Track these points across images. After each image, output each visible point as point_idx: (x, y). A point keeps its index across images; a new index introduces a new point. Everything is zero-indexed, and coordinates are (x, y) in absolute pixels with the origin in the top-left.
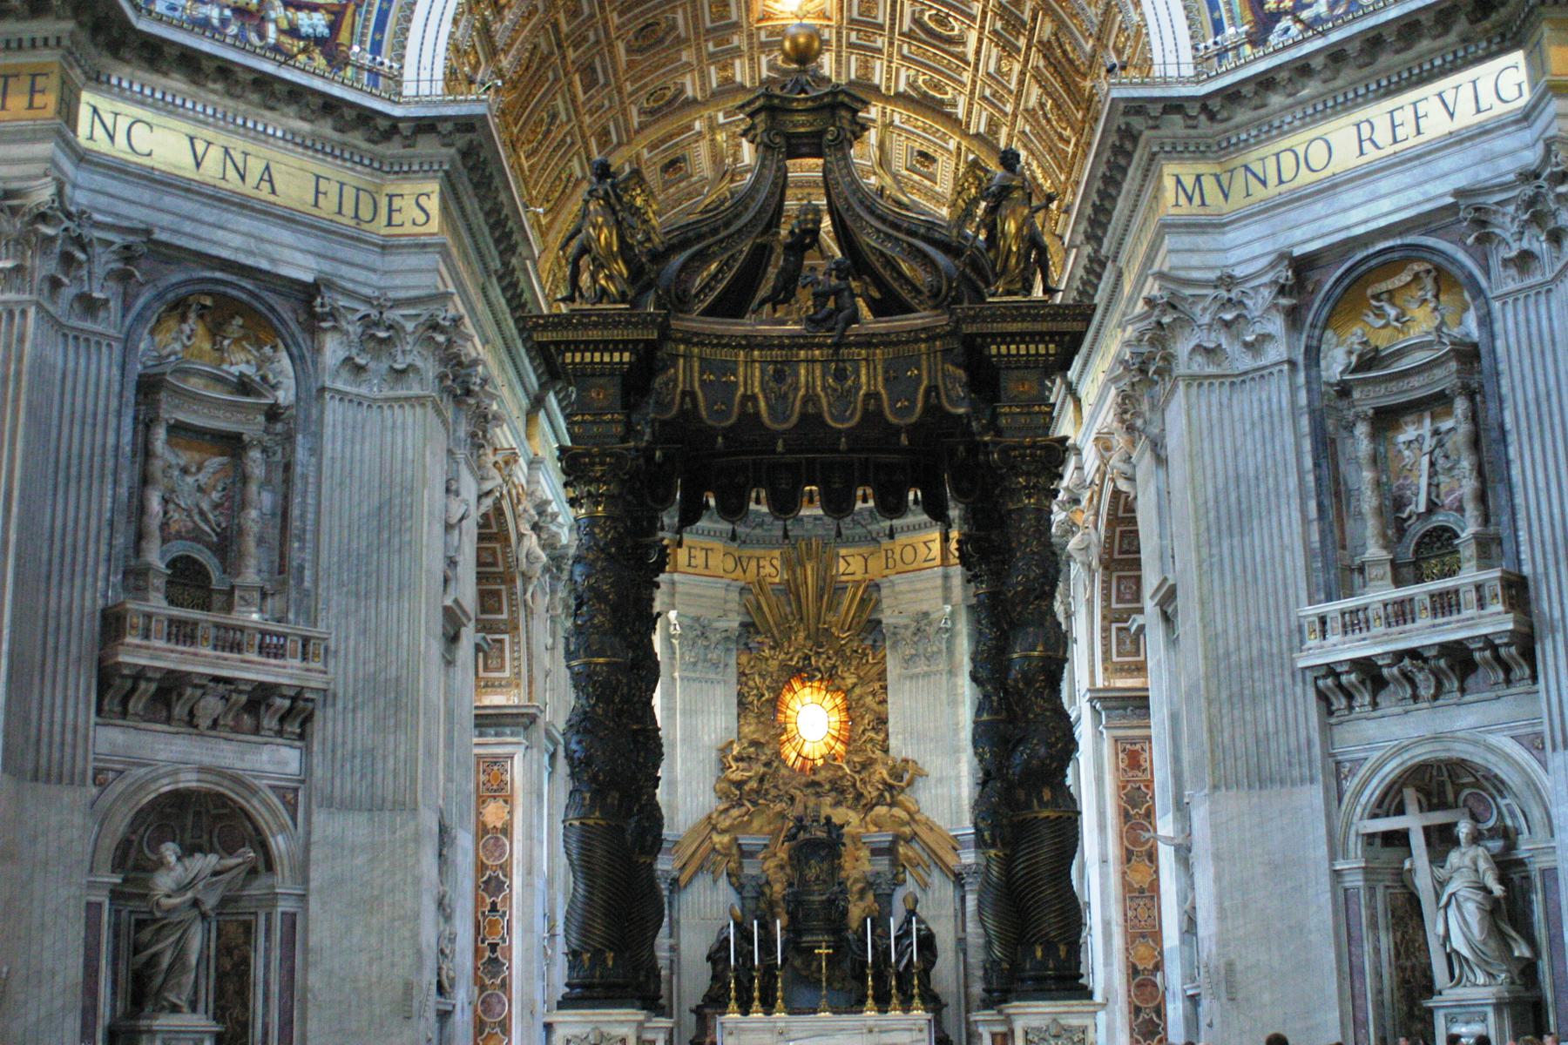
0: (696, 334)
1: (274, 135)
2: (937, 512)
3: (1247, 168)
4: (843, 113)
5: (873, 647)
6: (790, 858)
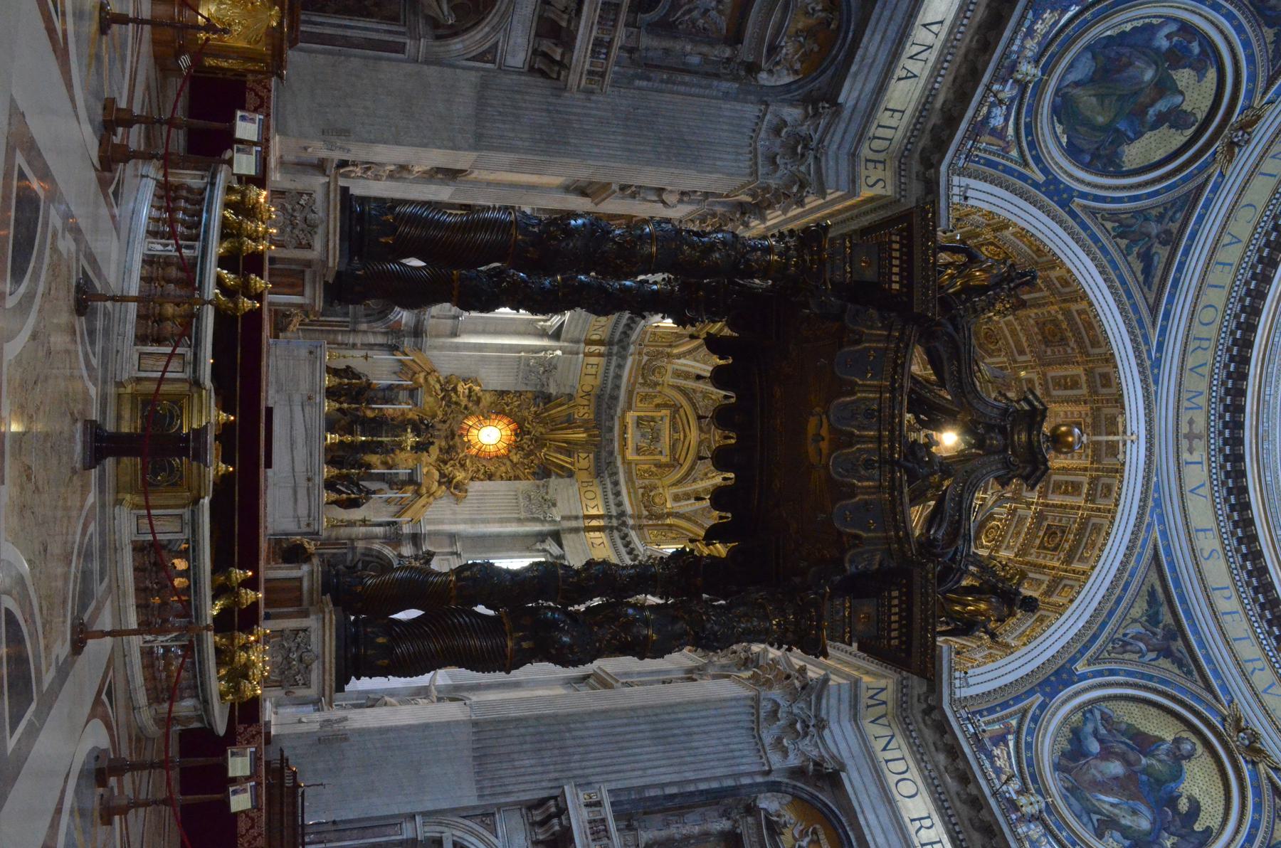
0: (907, 346)
1: (936, 82)
2: (713, 534)
3: (893, 736)
5: (534, 474)
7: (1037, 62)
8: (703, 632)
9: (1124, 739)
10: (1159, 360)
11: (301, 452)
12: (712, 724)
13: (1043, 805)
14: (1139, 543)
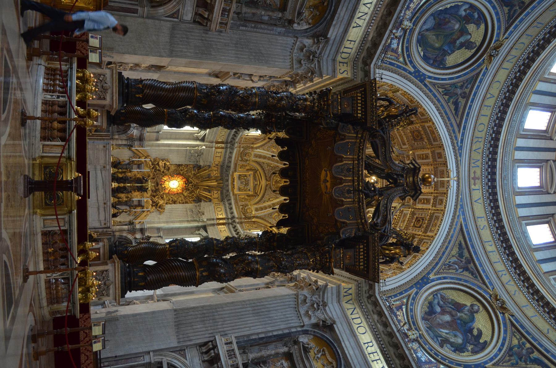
0: (364, 141)
1: (369, 29)
2: (280, 224)
3: (355, 308)
4: (413, 193)
5: (194, 201)
6: (138, 178)
7: (411, 20)
8: (281, 266)
9: (450, 306)
10: (461, 146)
11: (101, 191)
12: (278, 306)
13: (418, 335)
14: (455, 223)
